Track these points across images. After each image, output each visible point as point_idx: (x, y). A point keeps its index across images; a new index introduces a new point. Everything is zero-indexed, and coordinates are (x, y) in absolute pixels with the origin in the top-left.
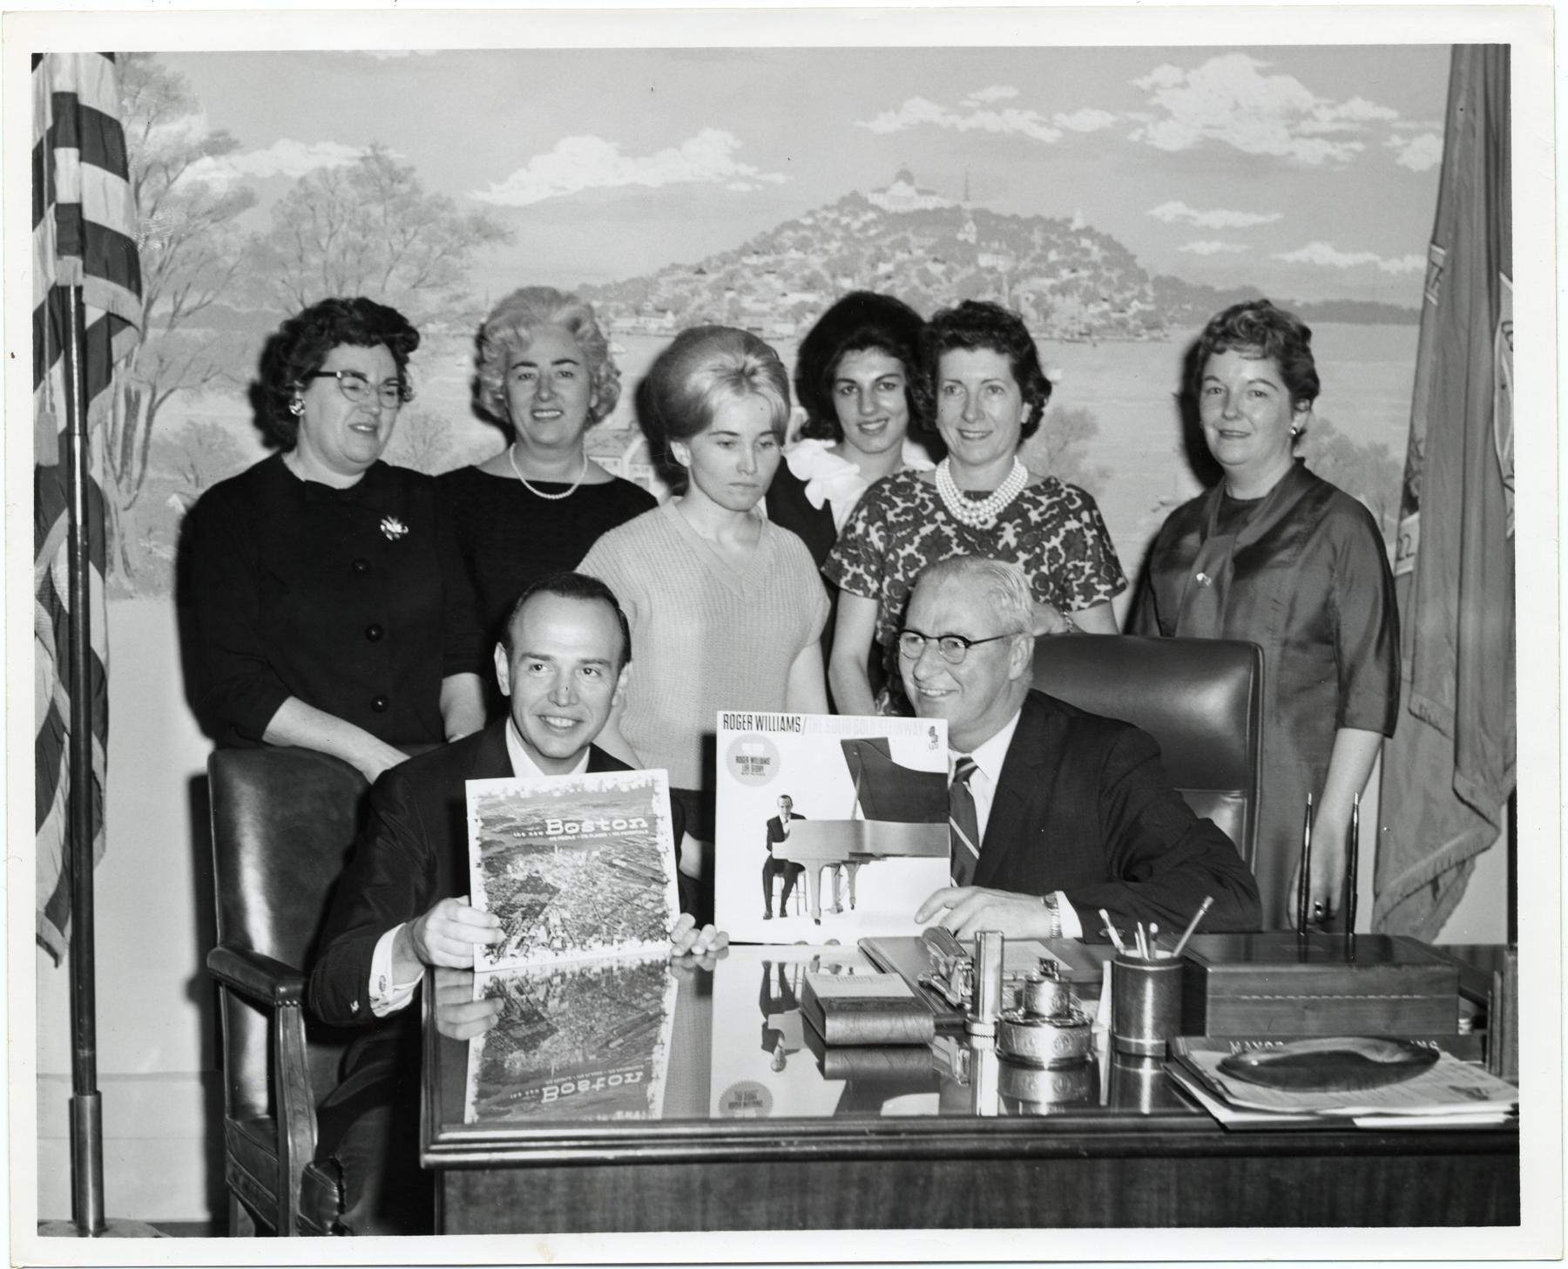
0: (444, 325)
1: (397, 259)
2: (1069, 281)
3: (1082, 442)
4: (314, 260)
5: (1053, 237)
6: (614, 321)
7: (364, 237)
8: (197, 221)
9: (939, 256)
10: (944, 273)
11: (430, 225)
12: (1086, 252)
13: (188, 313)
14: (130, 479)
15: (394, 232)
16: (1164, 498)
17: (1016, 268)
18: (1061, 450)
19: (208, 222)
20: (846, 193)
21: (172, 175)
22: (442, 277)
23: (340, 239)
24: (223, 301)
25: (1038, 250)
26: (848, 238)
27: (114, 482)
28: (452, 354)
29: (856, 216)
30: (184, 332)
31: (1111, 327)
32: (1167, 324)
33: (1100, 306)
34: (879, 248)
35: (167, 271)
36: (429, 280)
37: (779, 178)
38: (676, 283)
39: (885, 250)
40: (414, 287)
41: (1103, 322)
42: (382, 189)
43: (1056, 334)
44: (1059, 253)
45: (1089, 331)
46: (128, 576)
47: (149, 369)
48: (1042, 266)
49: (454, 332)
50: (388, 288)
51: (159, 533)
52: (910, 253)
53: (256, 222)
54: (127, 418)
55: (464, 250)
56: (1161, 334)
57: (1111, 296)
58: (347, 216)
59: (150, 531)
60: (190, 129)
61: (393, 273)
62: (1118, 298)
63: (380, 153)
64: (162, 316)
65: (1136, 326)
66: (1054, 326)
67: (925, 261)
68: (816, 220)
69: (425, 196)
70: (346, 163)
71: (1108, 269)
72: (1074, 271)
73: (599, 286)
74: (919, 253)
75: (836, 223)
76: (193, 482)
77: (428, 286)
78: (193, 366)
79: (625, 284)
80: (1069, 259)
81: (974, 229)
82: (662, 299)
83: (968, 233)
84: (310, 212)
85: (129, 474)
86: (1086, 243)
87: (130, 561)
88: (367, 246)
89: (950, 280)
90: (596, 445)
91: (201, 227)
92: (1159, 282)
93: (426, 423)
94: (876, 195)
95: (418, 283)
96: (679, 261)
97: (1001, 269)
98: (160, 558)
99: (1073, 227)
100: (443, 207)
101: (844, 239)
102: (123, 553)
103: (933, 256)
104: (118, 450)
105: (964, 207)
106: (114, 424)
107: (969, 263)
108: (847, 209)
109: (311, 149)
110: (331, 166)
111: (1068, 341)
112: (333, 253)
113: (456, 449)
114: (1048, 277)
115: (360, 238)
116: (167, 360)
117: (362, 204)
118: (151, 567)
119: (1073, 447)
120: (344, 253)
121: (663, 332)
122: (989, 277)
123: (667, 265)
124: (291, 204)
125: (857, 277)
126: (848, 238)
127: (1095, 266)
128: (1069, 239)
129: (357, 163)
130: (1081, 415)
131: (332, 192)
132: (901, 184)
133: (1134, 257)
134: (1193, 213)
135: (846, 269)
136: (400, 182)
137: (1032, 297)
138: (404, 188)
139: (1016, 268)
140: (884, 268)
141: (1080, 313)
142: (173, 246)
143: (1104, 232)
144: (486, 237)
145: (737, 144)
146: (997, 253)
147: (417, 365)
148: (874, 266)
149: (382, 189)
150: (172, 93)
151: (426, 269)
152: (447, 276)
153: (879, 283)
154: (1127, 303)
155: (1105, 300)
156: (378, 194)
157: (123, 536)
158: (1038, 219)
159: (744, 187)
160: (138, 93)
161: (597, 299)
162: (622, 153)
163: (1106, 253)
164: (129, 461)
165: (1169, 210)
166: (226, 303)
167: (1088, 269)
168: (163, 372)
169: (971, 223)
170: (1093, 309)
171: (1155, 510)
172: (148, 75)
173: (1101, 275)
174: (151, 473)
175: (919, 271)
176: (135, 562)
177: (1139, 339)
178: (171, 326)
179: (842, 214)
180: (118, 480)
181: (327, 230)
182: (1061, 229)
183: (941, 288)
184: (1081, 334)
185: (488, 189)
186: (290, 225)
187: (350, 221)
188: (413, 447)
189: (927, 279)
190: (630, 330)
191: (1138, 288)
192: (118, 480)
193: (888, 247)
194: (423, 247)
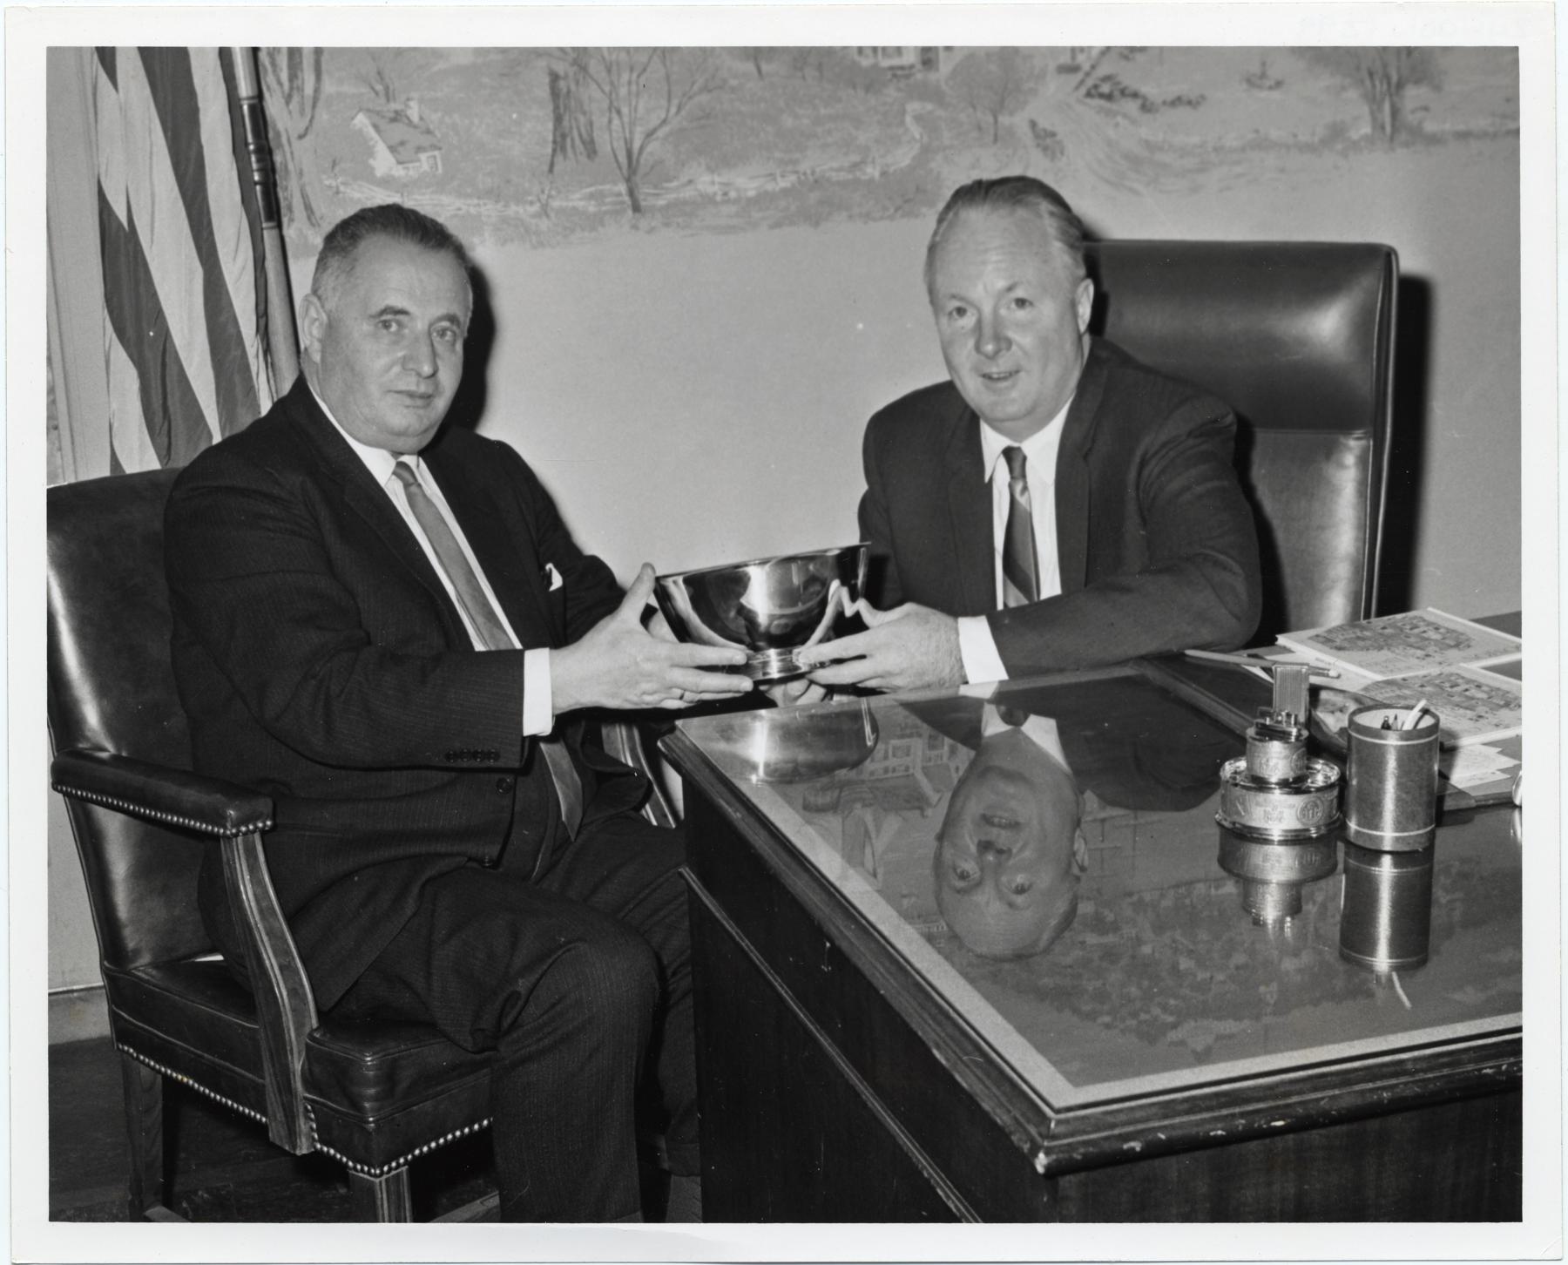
14: (303, 97)
27: (283, 101)
46: (313, 225)
59: (334, 164)
76: (382, 93)
85: (301, 90)
87: (314, 206)
102: (304, 196)
157: (301, 174)
164: (299, 74)
174: (329, 87)
176: (320, 207)
180: (288, 99)
192: (288, 99)
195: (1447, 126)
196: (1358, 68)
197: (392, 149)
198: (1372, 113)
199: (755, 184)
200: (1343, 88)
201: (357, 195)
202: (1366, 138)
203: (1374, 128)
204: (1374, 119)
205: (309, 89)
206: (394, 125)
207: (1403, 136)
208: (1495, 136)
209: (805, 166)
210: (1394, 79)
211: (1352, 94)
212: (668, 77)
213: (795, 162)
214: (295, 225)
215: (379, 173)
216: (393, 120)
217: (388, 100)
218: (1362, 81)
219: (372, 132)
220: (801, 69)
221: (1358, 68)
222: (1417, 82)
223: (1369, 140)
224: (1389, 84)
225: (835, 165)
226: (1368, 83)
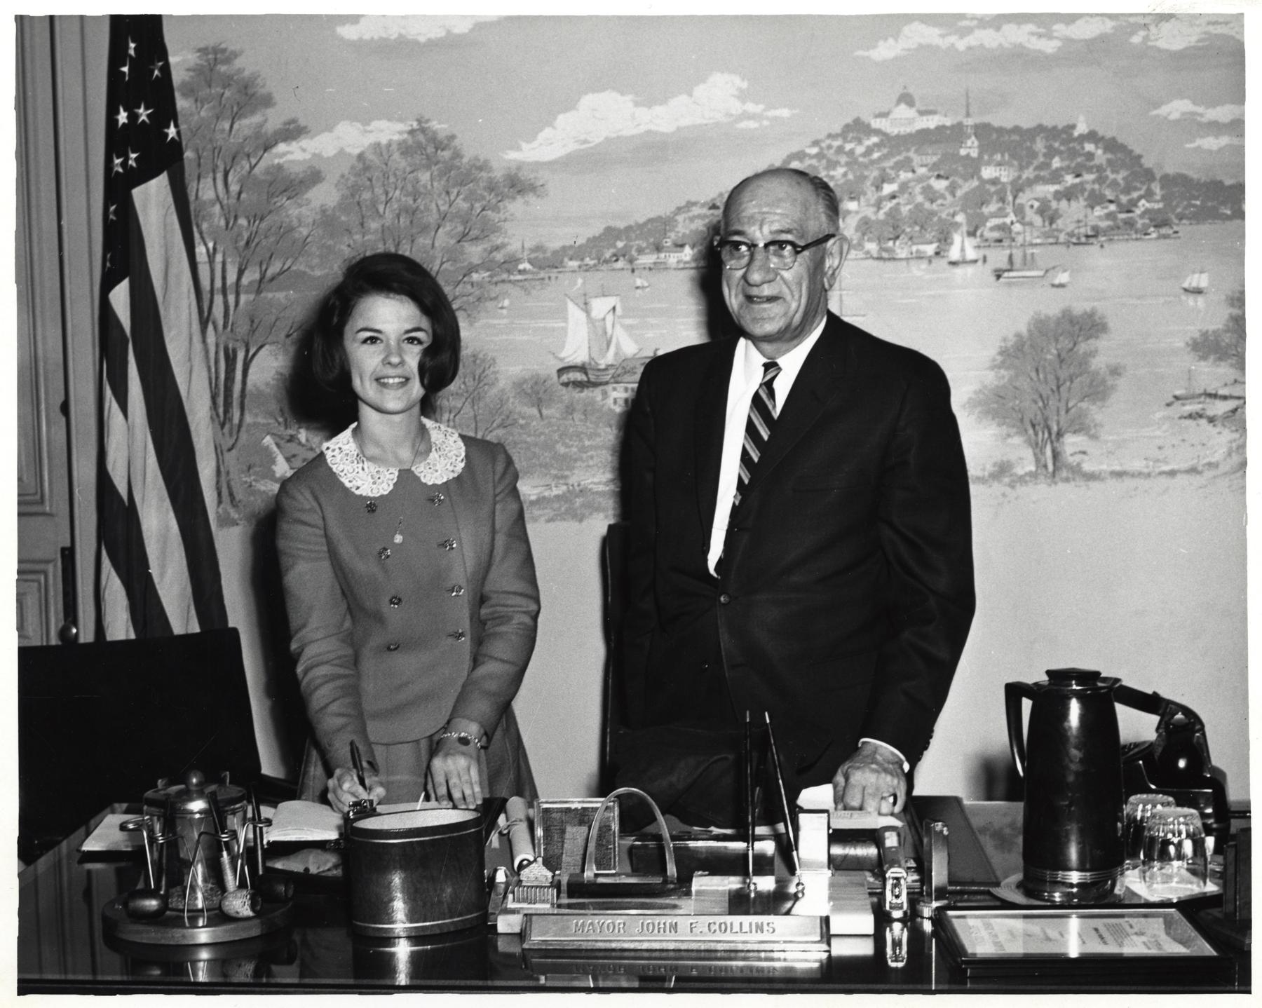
0: (488, 274)
1: (444, 219)
2: (1074, 186)
3: (1092, 341)
4: (374, 225)
5: (1056, 145)
6: (637, 259)
7: (415, 200)
8: (276, 199)
9: (942, 173)
10: (947, 188)
11: (471, 185)
12: (1090, 156)
13: (272, 279)
14: (232, 425)
15: (440, 195)
16: (1178, 393)
17: (1020, 177)
18: (1071, 350)
19: (285, 199)
20: (849, 120)
21: (253, 161)
22: (483, 231)
23: (396, 206)
24: (300, 266)
25: (1041, 159)
26: (852, 163)
28: (495, 298)
29: (860, 142)
30: (270, 295)
31: (1119, 228)
32: (1176, 221)
33: (1106, 208)
34: (884, 170)
35: (254, 244)
36: (474, 233)
37: (785, 113)
38: (692, 219)
39: (888, 171)
40: (459, 241)
41: (1109, 223)
42: (428, 158)
43: (1062, 238)
44: (1062, 160)
45: (1096, 233)
47: (243, 328)
48: (1042, 173)
49: (495, 279)
50: (437, 244)
51: (257, 469)
52: (914, 171)
53: (324, 196)
54: (227, 372)
55: (501, 204)
56: (1171, 232)
57: (1117, 196)
58: (400, 184)
59: (249, 468)
60: (266, 121)
61: (440, 230)
62: (1124, 199)
63: (423, 125)
64: (251, 283)
65: (1143, 224)
66: (1060, 231)
67: (929, 178)
68: (821, 149)
69: (465, 160)
70: (396, 137)
71: (1113, 172)
72: (1078, 176)
73: (621, 225)
74: (922, 171)
75: (840, 150)
77: (472, 240)
78: (278, 323)
79: (645, 224)
80: (1073, 165)
81: (976, 143)
82: (680, 235)
83: (971, 148)
84: (368, 183)
85: (231, 420)
86: (1089, 147)
87: (235, 494)
88: (418, 207)
89: (954, 196)
90: (625, 373)
91: (279, 204)
92: (1167, 181)
93: (474, 362)
94: (878, 120)
95: (463, 237)
96: (693, 200)
97: (1004, 180)
98: (259, 491)
99: (1076, 134)
100: (481, 169)
101: (847, 164)
102: (229, 487)
103: (936, 173)
104: (221, 400)
105: (965, 123)
106: (217, 378)
107: (972, 177)
108: (851, 135)
109: (369, 128)
110: (384, 141)
111: (1075, 244)
112: (389, 215)
113: (502, 384)
114: (1053, 183)
115: (411, 202)
116: (256, 321)
117: (412, 172)
118: (252, 498)
119: (1083, 347)
120: (398, 216)
121: (681, 265)
122: (993, 189)
123: (683, 204)
124: (352, 178)
125: (862, 199)
126: (852, 163)
127: (1100, 169)
128: (1071, 145)
129: (406, 136)
130: (1091, 315)
131: (386, 164)
132: (903, 106)
133: (1140, 157)
134: (1200, 110)
135: (851, 193)
136: (443, 150)
137: (1036, 204)
138: (446, 154)
139: (1020, 177)
140: (888, 189)
141: (1086, 216)
142: (257, 222)
143: (1109, 135)
144: (519, 192)
145: (745, 85)
146: (999, 164)
147: (465, 310)
148: (878, 188)
149: (427, 155)
150: (250, 91)
151: (469, 225)
152: (488, 230)
153: (884, 203)
154: (1134, 203)
155: (1111, 202)
156: (424, 162)
157: (228, 473)
158: (1040, 129)
159: (752, 125)
160: (223, 94)
161: (621, 240)
162: (637, 104)
163: (1109, 156)
165: (1177, 108)
166: (302, 268)
167: (1092, 173)
168: (254, 331)
169: (973, 138)
170: (1099, 211)
171: (1168, 405)
172: (230, 77)
173: (1107, 177)
174: (248, 419)
175: (923, 187)
177: (1147, 237)
178: (259, 291)
179: (845, 140)
181: (383, 198)
182: (1064, 136)
183: (944, 202)
184: (1087, 236)
185: (519, 149)
186: (353, 195)
187: (403, 188)
188: (464, 383)
189: (932, 196)
190: (652, 266)
191: (1145, 188)
193: (892, 168)
194: (465, 206)
195: (1104, 467)
196: (1022, 420)
197: (288, 460)
198: (1035, 454)
199: (536, 491)
200: (1009, 436)
201: (263, 488)
202: (1030, 474)
203: (1037, 467)
204: (1037, 460)
205: (236, 420)
206: (289, 444)
207: (1064, 474)
208: (1149, 475)
209: (573, 480)
210: (1055, 429)
211: (1017, 440)
212: (475, 416)
213: (566, 477)
214: (222, 506)
215: (278, 475)
216: (289, 441)
217: (286, 428)
218: (1026, 431)
219: (275, 448)
220: (571, 414)
221: (1022, 420)
222: (1075, 432)
223: (1033, 475)
224: (1050, 434)
225: (596, 480)
226: (1031, 431)
